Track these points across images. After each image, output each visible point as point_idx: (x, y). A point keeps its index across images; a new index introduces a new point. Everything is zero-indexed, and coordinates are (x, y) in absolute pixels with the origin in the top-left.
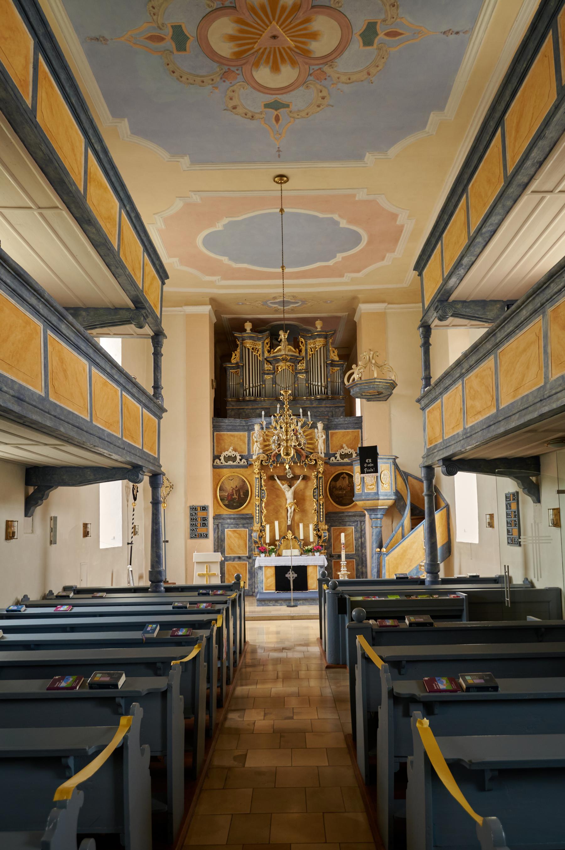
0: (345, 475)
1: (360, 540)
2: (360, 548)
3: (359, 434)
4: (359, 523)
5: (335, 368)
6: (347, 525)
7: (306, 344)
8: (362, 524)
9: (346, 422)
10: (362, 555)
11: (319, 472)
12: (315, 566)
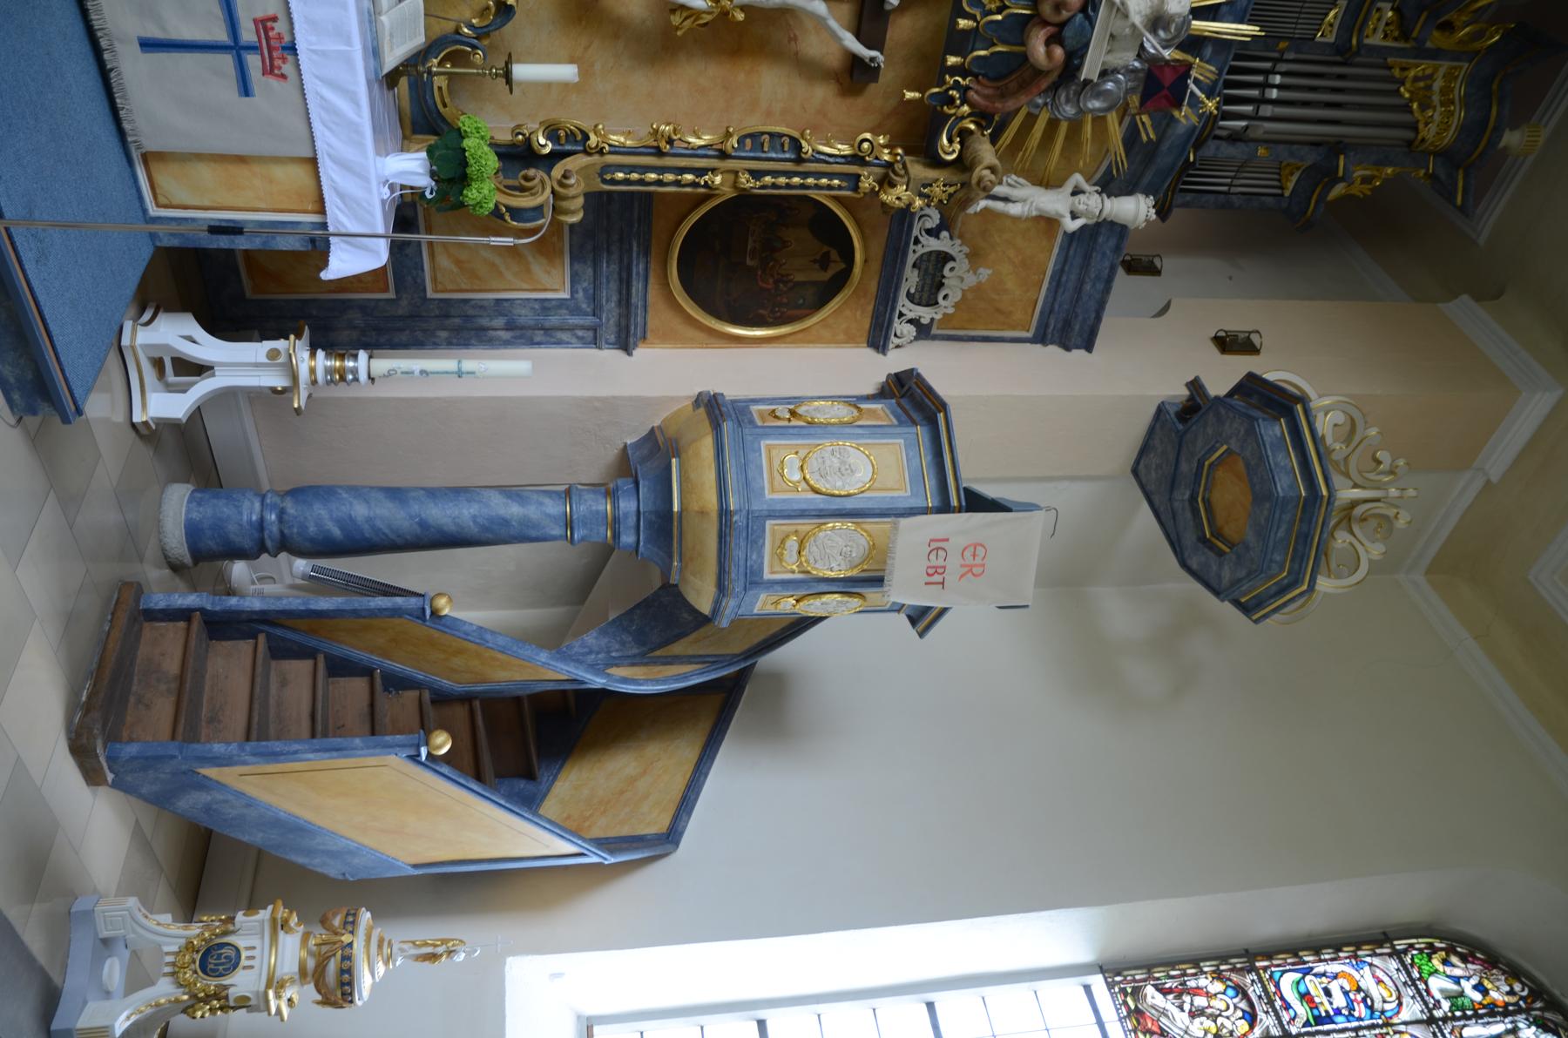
0: (837, 266)
1: (499, 322)
2: (457, 321)
3: (1013, 328)
4: (589, 320)
5: (1294, 178)
6: (577, 266)
7: (1455, 56)
8: (580, 333)
9: (1088, 287)
10: (425, 331)
11: (886, 182)
12: (321, 200)
